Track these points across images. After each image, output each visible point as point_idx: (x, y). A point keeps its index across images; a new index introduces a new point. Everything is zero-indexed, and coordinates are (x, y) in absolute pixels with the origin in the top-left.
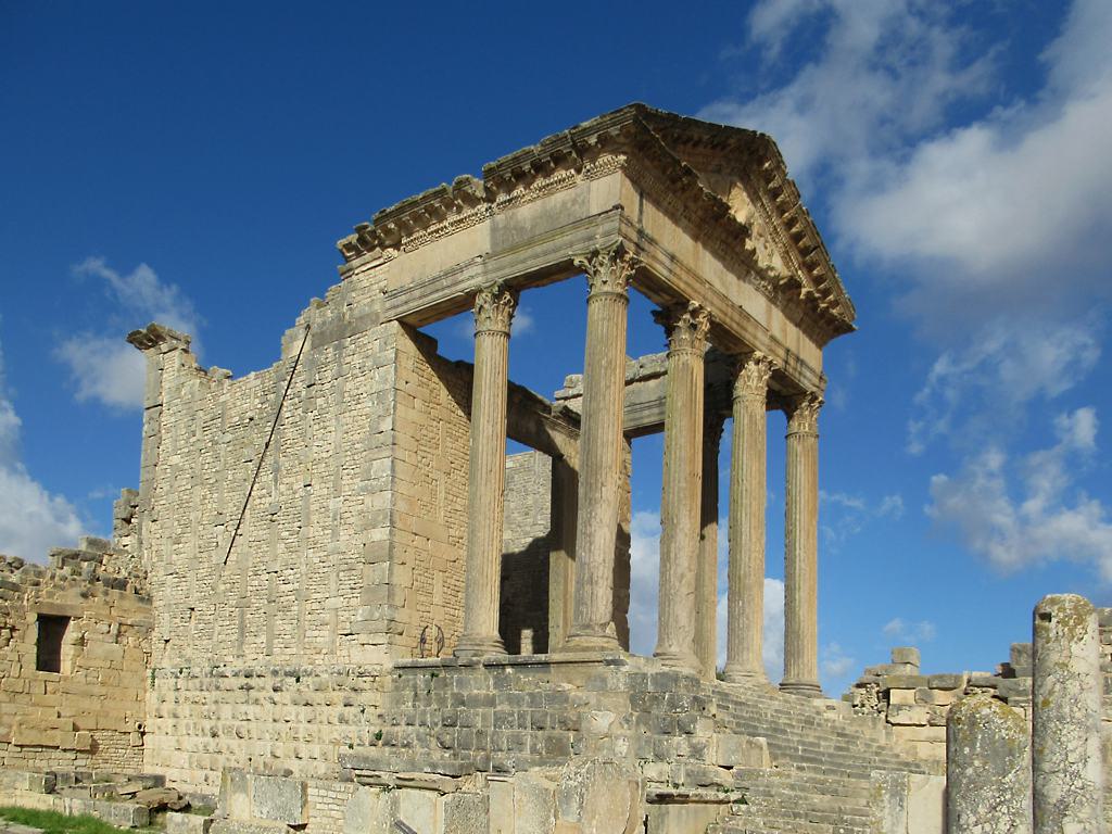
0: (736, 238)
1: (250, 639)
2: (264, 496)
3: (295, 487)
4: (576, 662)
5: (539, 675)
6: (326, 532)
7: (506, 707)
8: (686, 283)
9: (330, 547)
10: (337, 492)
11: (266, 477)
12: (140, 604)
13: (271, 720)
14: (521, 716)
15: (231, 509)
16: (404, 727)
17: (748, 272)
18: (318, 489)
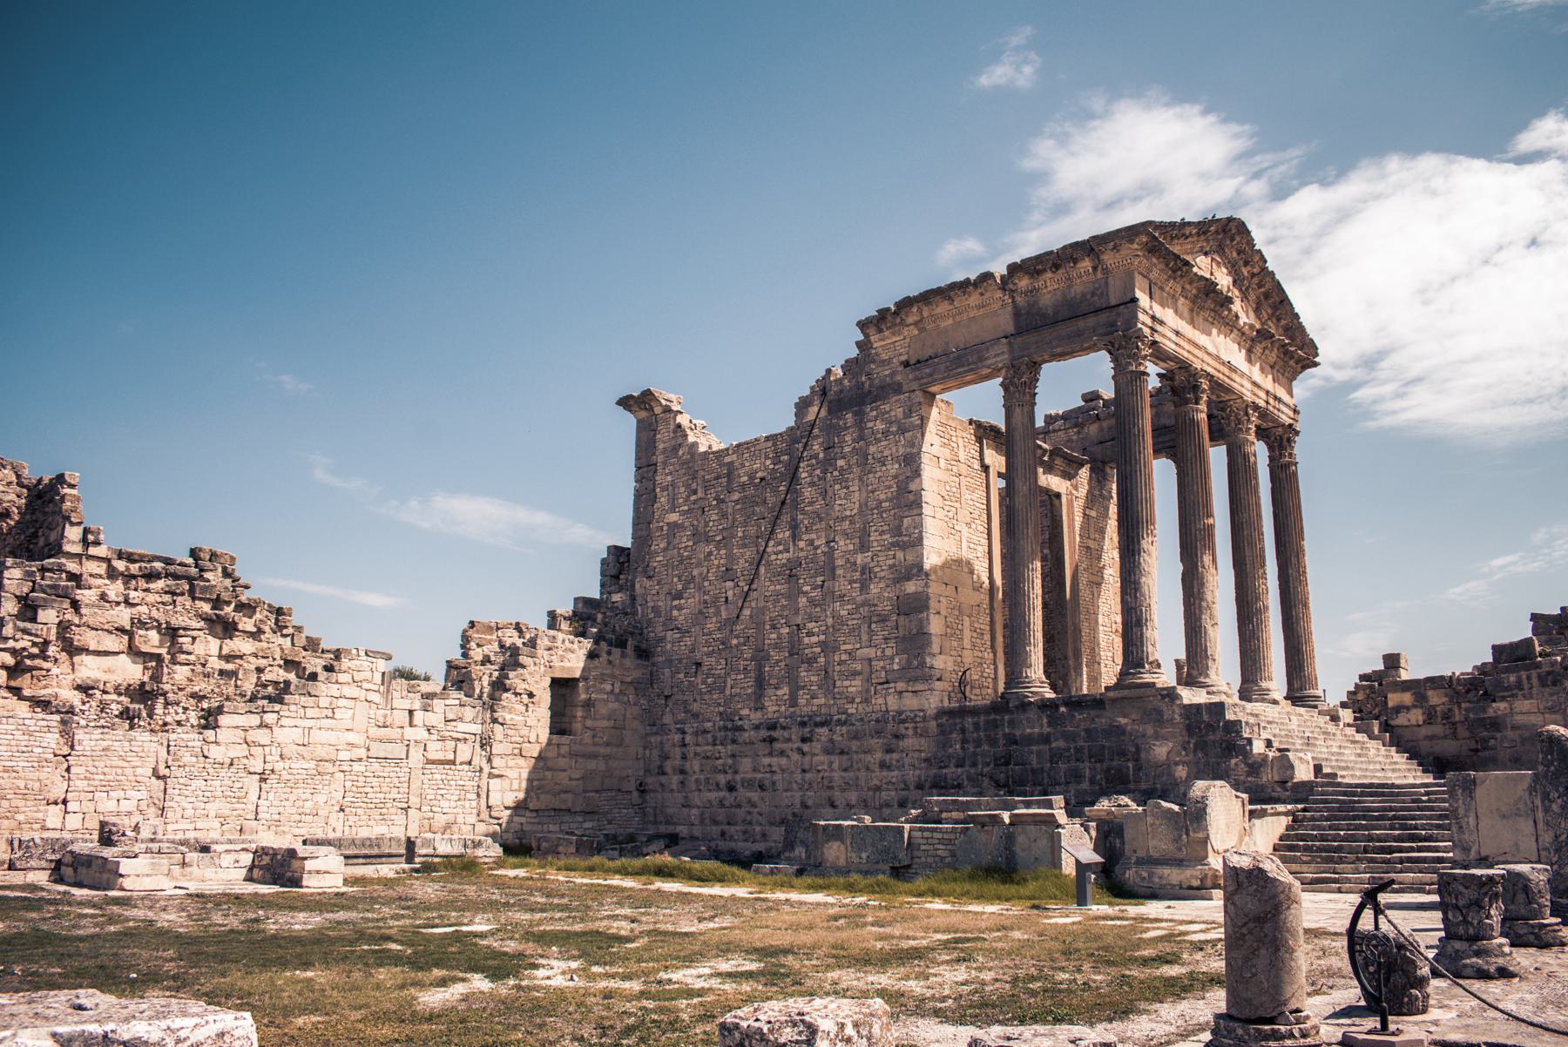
0: (1222, 306)
1: (770, 691)
2: (781, 552)
3: (817, 543)
4: (1131, 698)
5: (1093, 713)
6: (855, 585)
7: (1061, 744)
8: (1189, 352)
9: (859, 599)
10: (864, 547)
11: (783, 534)
12: (639, 662)
13: (799, 771)
14: (1078, 750)
15: (741, 565)
16: (954, 769)
17: (1232, 331)
18: (842, 545)
